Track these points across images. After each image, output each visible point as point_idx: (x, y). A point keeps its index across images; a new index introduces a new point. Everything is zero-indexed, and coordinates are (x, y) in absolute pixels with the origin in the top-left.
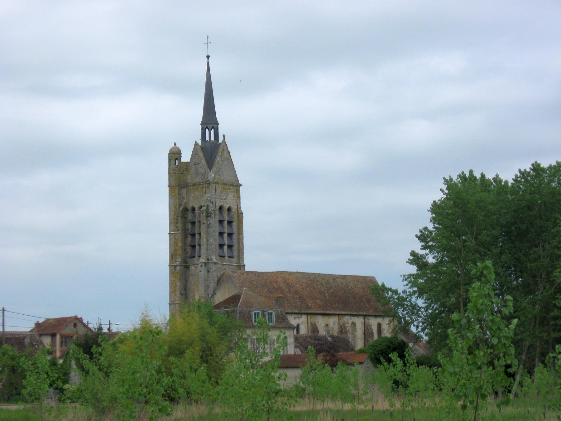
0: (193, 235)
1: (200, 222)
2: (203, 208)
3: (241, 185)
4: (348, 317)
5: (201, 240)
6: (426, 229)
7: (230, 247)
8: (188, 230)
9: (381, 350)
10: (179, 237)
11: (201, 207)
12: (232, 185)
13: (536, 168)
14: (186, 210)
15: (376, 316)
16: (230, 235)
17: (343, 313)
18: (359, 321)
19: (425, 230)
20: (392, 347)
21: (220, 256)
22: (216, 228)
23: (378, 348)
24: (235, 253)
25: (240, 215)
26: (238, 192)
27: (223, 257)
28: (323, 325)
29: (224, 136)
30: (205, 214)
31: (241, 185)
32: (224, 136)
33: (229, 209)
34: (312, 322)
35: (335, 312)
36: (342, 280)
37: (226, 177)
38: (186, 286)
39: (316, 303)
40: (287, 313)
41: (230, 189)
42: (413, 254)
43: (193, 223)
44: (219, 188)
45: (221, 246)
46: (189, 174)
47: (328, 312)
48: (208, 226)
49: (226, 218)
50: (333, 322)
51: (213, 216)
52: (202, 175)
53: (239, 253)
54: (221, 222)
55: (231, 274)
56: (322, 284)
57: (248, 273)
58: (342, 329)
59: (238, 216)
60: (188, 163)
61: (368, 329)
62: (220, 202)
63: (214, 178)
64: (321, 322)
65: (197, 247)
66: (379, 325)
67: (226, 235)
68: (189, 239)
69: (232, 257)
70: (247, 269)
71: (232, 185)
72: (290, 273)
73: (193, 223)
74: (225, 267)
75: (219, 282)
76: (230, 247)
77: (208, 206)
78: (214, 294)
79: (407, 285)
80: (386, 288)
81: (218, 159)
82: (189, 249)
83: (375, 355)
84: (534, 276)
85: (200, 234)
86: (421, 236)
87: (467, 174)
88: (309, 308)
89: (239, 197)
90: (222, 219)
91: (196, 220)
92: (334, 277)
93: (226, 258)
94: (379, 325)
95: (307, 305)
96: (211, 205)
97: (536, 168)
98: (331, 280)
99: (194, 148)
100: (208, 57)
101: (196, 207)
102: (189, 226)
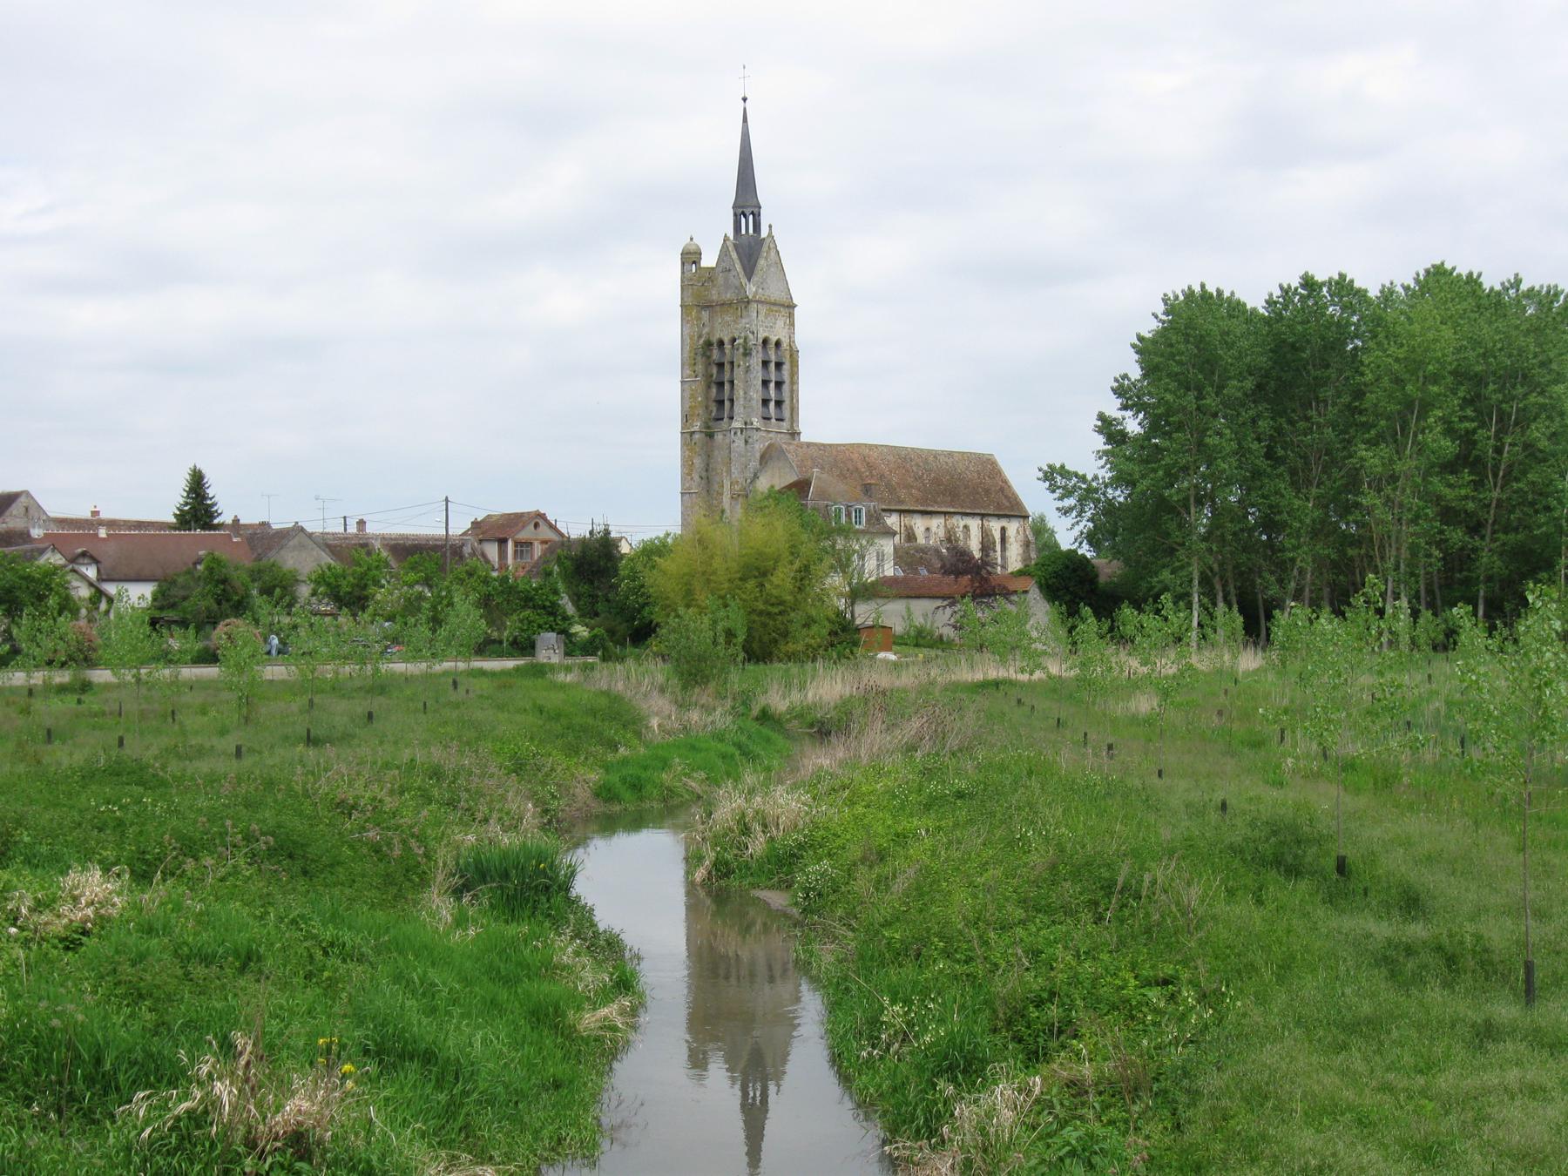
0: (721, 385)
1: (732, 363)
2: (737, 341)
3: (796, 306)
4: (959, 517)
5: (735, 392)
6: (1125, 377)
7: (779, 403)
8: (712, 376)
9: (1055, 572)
10: (699, 387)
11: (734, 340)
12: (783, 305)
13: (1308, 283)
14: (709, 344)
15: (999, 516)
16: (779, 384)
17: (952, 510)
18: (974, 524)
19: (1123, 379)
20: (1071, 567)
21: (764, 418)
22: (758, 374)
23: (1050, 569)
24: (786, 413)
25: (794, 354)
26: (791, 316)
27: (769, 419)
28: (923, 529)
29: (770, 226)
30: (741, 350)
31: (796, 306)
32: (770, 226)
33: (778, 344)
34: (907, 524)
35: (939, 510)
36: (946, 460)
37: (774, 293)
38: (708, 465)
39: (911, 494)
40: (884, 510)
41: (780, 312)
42: (1101, 417)
43: (721, 365)
44: (763, 309)
45: (765, 402)
46: (714, 286)
47: (930, 509)
48: (748, 370)
49: (773, 358)
50: (937, 524)
51: (754, 353)
52: (736, 288)
53: (792, 414)
54: (765, 364)
55: (784, 446)
56: (917, 465)
57: (809, 445)
58: (950, 537)
59: (791, 356)
60: (713, 268)
61: (987, 535)
62: (764, 331)
63: (756, 293)
64: (919, 524)
65: (727, 404)
66: (1003, 530)
67: (772, 385)
68: (714, 390)
69: (782, 420)
70: (804, 438)
71: (783, 305)
72: (870, 447)
73: (721, 365)
74: (771, 435)
75: (765, 458)
76: (779, 403)
77: (745, 338)
78: (756, 477)
79: (1103, 467)
80: (1068, 472)
81: (762, 262)
82: (714, 408)
83: (1046, 579)
84: (1305, 457)
85: (732, 382)
86: (1118, 388)
87: (1197, 289)
88: (902, 502)
89: (792, 324)
90: (766, 359)
91: (726, 360)
92: (936, 455)
93: (773, 420)
94: (1003, 530)
95: (899, 497)
96: (751, 336)
97: (1308, 283)
98: (931, 458)
99: (723, 247)
100: (745, 99)
101: (726, 340)
102: (715, 370)
